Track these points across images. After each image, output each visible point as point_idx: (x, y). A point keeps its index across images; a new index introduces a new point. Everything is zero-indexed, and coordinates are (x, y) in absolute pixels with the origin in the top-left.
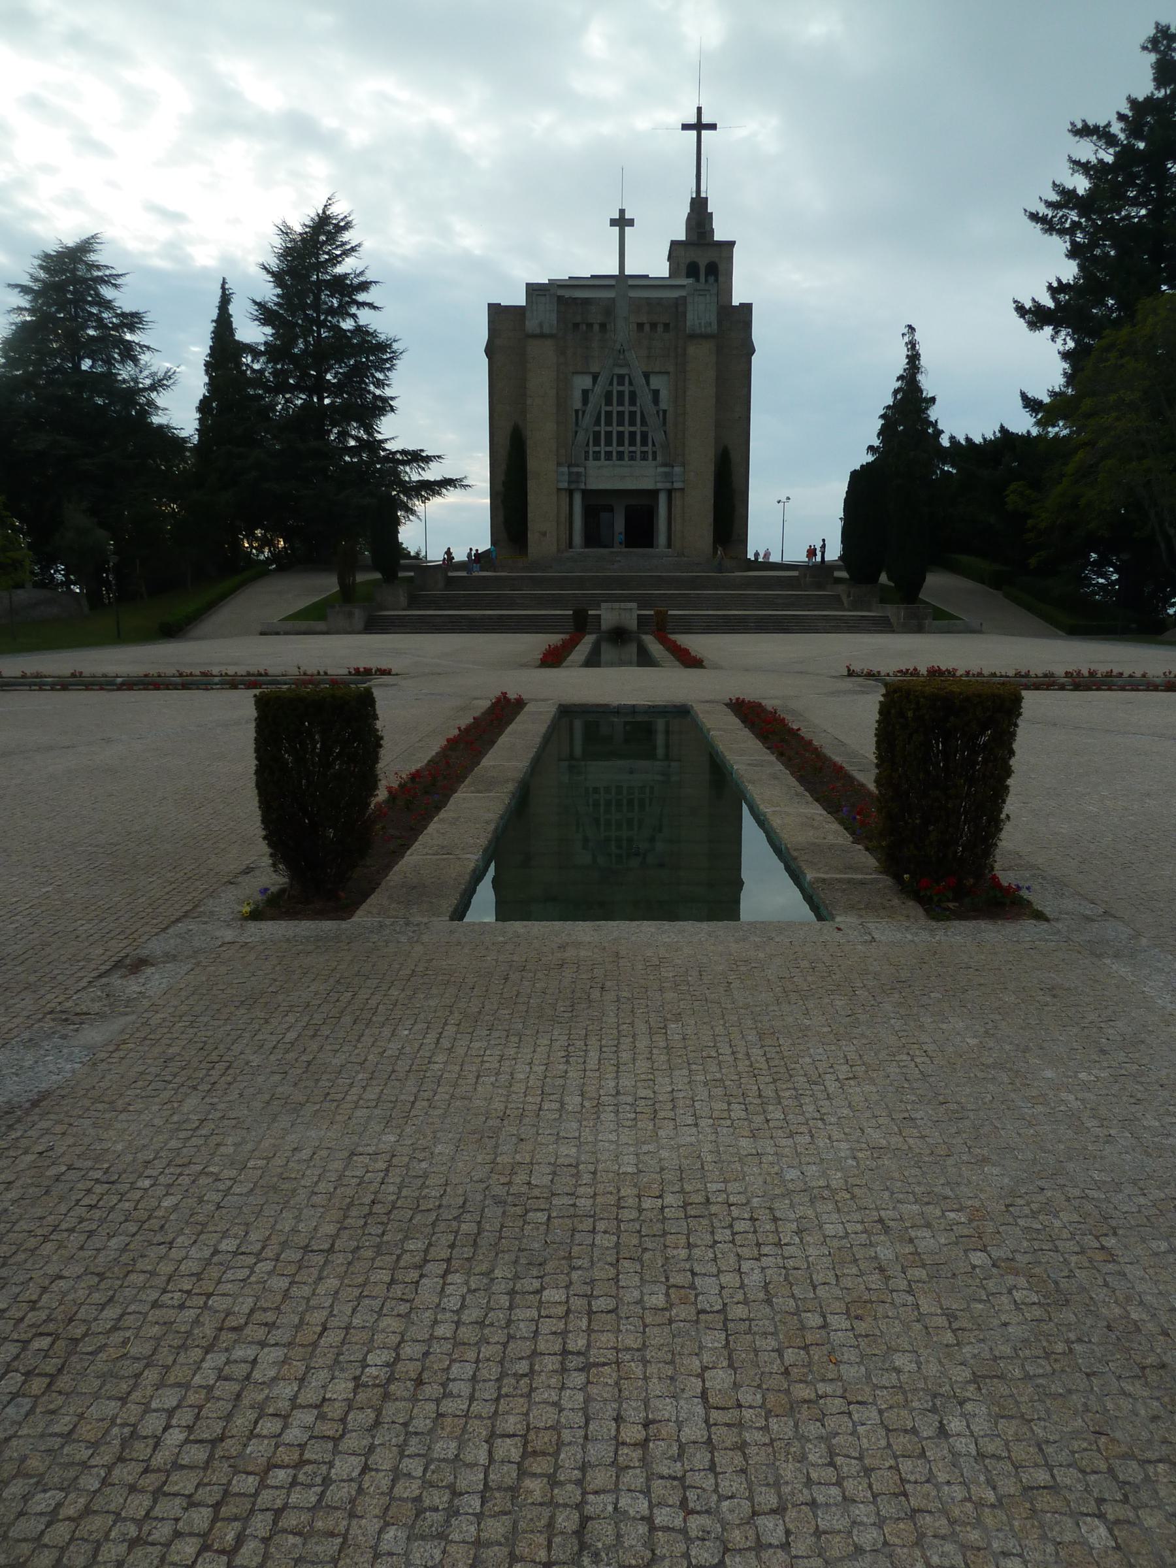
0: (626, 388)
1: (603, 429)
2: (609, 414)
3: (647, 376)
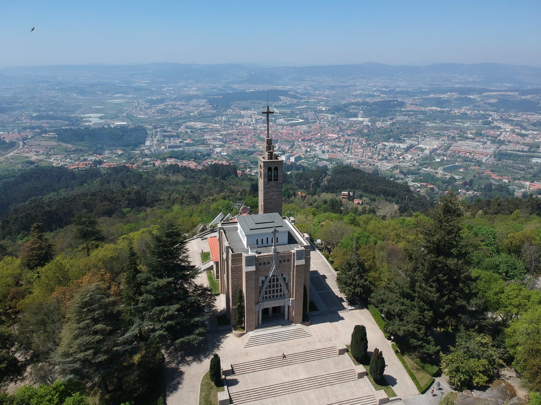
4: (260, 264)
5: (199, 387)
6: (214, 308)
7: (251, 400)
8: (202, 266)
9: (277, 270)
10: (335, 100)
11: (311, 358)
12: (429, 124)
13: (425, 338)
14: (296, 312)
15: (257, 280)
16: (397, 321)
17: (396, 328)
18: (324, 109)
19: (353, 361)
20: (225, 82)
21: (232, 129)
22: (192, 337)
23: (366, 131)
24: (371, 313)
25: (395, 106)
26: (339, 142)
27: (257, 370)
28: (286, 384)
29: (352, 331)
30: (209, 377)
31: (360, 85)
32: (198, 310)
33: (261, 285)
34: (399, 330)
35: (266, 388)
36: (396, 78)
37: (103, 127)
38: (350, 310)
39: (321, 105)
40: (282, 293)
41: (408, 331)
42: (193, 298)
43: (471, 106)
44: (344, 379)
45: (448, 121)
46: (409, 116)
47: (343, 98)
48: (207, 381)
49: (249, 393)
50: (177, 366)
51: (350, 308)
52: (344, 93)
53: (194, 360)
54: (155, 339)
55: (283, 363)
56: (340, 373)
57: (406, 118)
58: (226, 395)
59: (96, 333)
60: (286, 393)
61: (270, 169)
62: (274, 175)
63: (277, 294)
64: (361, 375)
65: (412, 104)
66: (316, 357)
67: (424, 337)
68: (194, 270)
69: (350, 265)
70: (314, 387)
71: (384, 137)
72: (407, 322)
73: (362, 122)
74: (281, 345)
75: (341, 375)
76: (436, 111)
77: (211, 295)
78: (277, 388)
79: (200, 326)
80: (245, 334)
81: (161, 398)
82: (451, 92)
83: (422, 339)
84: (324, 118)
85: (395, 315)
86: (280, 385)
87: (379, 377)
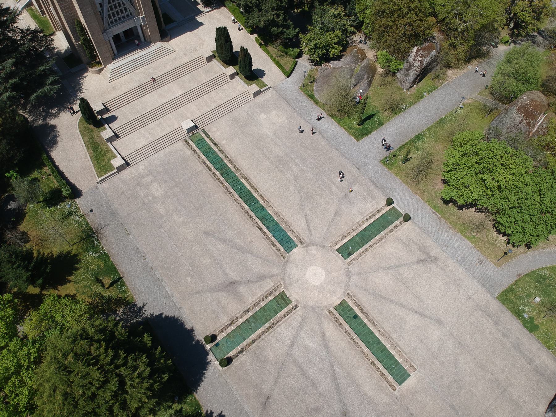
2: (111, 7)
5: (79, 133)
6: (56, 50)
7: (136, 129)
11: (181, 73)
13: (285, 23)
16: (256, 13)
22: (46, 88)
27: (131, 101)
28: (165, 105)
30: (84, 121)
32: (39, 58)
35: (146, 114)
42: (26, 46)
44: (218, 84)
48: (84, 126)
49: (131, 124)
50: (44, 122)
55: (155, 86)
56: (213, 80)
58: (110, 132)
60: (167, 113)
66: (186, 71)
67: (283, 22)
68: (11, 13)
70: (192, 100)
75: (214, 82)
77: (45, 36)
78: (157, 111)
79: (50, 74)
80: (103, 68)
83: (282, 26)
86: (159, 108)
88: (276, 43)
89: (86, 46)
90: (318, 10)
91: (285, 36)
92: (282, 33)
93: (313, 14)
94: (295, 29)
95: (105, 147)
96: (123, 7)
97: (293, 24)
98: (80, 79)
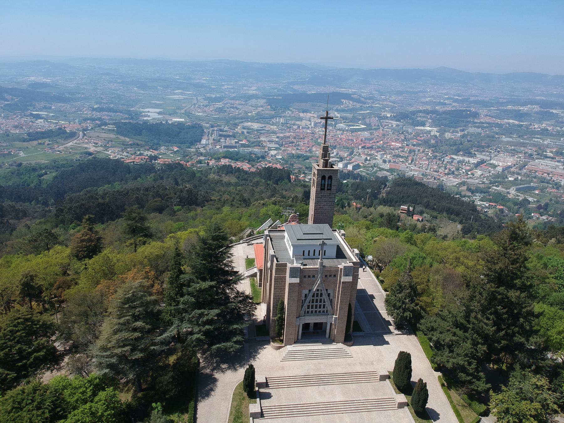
0: (320, 292)
1: (311, 304)
2: (313, 300)
3: (327, 290)
4: (305, 277)
5: (232, 396)
7: (283, 416)
8: (245, 272)
9: (322, 285)
10: (402, 106)
11: (350, 380)
12: (505, 139)
13: (476, 374)
14: (339, 330)
15: (300, 293)
16: (446, 352)
17: (444, 359)
18: (389, 115)
19: (395, 389)
20: (286, 83)
21: (289, 132)
23: (433, 142)
24: (419, 340)
25: (468, 116)
26: (403, 152)
27: (292, 386)
28: (320, 404)
29: (396, 357)
30: (242, 387)
31: (430, 91)
33: (304, 298)
34: (448, 362)
35: (299, 406)
36: (471, 85)
37: (161, 122)
38: (396, 334)
39: (386, 111)
40: (325, 309)
41: (458, 364)
43: (553, 122)
44: (383, 407)
45: (525, 137)
46: (483, 128)
47: (410, 105)
49: (281, 409)
51: (396, 332)
52: (412, 99)
53: (229, 368)
54: (192, 343)
55: (320, 382)
56: (379, 400)
57: (479, 130)
58: (258, 407)
59: (135, 330)
60: (319, 414)
61: (323, 178)
62: (328, 184)
63: (320, 309)
64: (401, 405)
65: (487, 115)
66: (355, 380)
67: (474, 372)
69: (401, 287)
70: (350, 411)
71: (452, 149)
72: (458, 354)
73: (429, 132)
74: (319, 363)
75: (380, 402)
76: (514, 125)
78: (310, 407)
81: (192, 403)
82: (532, 105)
83: (471, 375)
84: (388, 125)
85: (444, 345)
86: (314, 404)
87: (420, 409)
88: (460, 390)
89: (278, 323)
90: (518, 372)
91: (473, 387)
92: (470, 383)
93: (511, 376)
94: (486, 384)
95: (246, 420)
96: (322, 304)
97: (486, 377)
98: (260, 348)
